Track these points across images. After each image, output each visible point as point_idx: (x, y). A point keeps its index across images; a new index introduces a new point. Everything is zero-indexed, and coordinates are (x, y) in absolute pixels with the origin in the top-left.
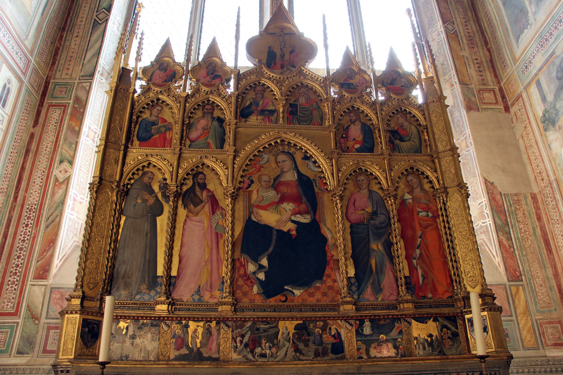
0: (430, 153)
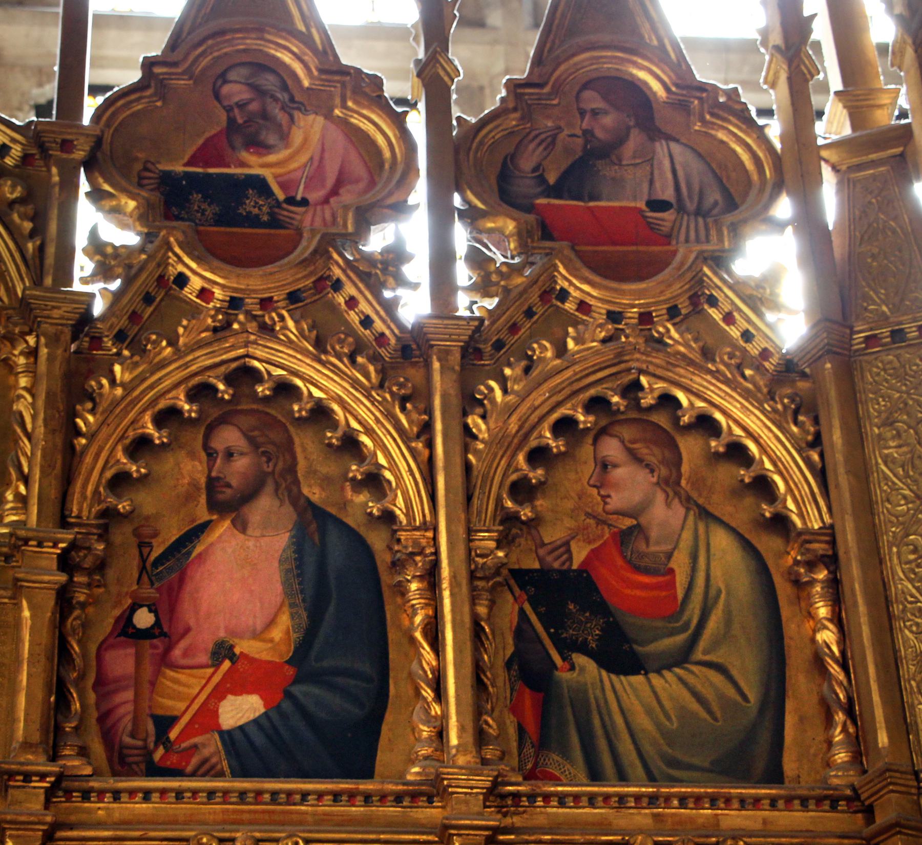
0: (853, 777)
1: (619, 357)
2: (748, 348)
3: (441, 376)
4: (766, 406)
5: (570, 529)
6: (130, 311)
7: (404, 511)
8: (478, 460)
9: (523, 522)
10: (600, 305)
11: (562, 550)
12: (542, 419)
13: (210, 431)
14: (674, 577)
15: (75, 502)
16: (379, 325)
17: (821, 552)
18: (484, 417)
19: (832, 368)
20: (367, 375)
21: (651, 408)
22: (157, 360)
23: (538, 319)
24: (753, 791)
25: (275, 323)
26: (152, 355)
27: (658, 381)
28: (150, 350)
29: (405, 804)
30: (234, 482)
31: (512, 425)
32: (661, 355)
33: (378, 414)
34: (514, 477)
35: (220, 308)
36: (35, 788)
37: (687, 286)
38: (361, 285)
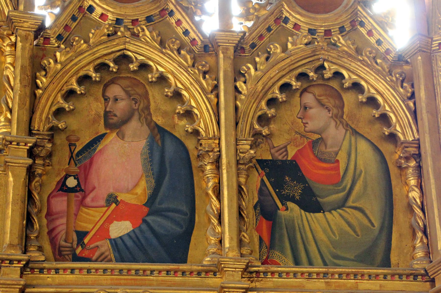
1: (314, 53)
2: (379, 49)
3: (224, 61)
4: (387, 78)
5: (287, 140)
6: (65, 25)
7: (204, 130)
8: (242, 105)
9: (264, 136)
10: (305, 26)
11: (283, 150)
12: (274, 84)
13: (106, 86)
14: (339, 164)
15: (36, 123)
16: (192, 35)
17: (412, 152)
18: (245, 82)
19: (421, 59)
20: (186, 61)
21: (329, 79)
22: (78, 51)
23: (273, 32)
24: (375, 271)
25: (139, 33)
26: (76, 48)
27: (333, 65)
28: (75, 45)
29: (202, 276)
30: (118, 114)
31: (259, 87)
32: (335, 52)
33: (191, 80)
34: (259, 113)
35: (112, 24)
36: (15, 267)
37: (349, 16)
38: (183, 14)
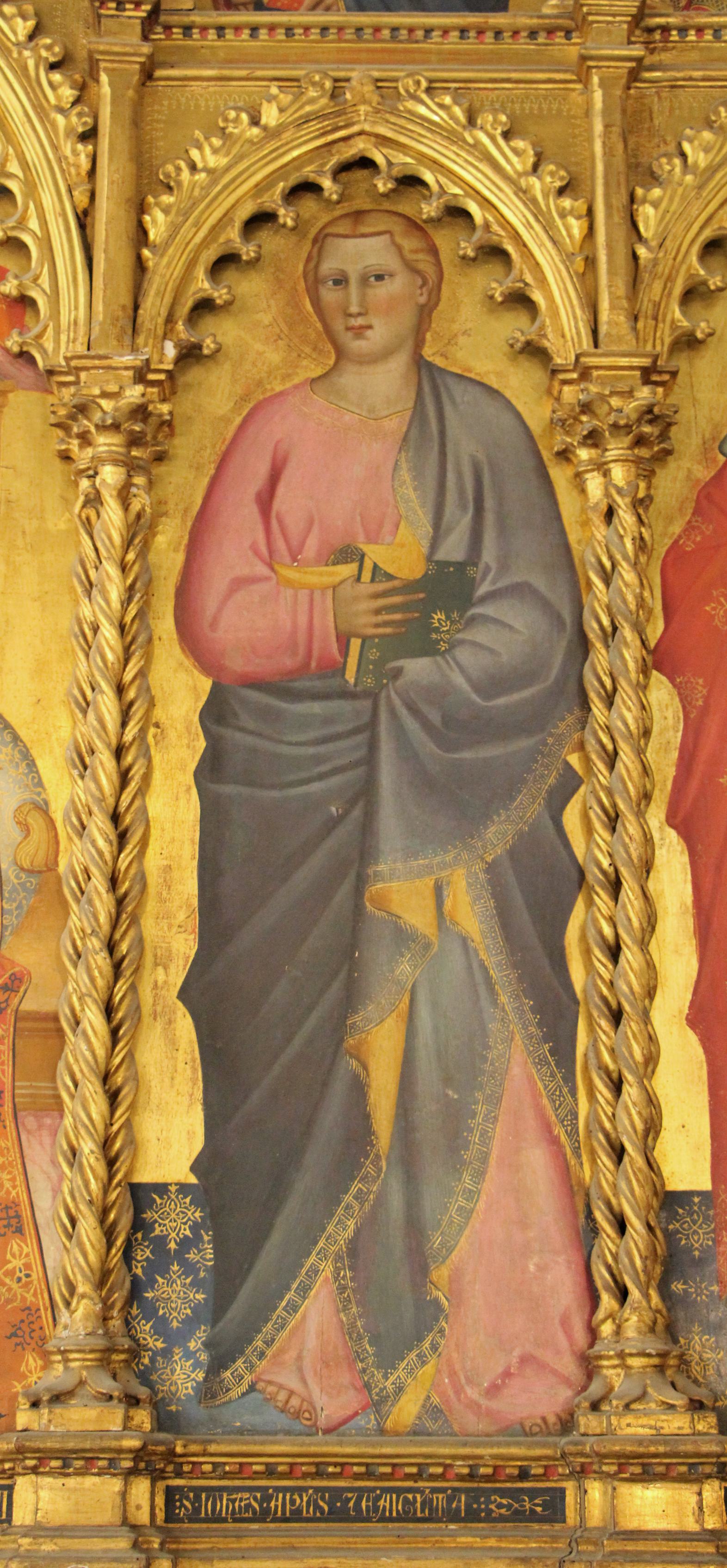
36: (130, 17)
